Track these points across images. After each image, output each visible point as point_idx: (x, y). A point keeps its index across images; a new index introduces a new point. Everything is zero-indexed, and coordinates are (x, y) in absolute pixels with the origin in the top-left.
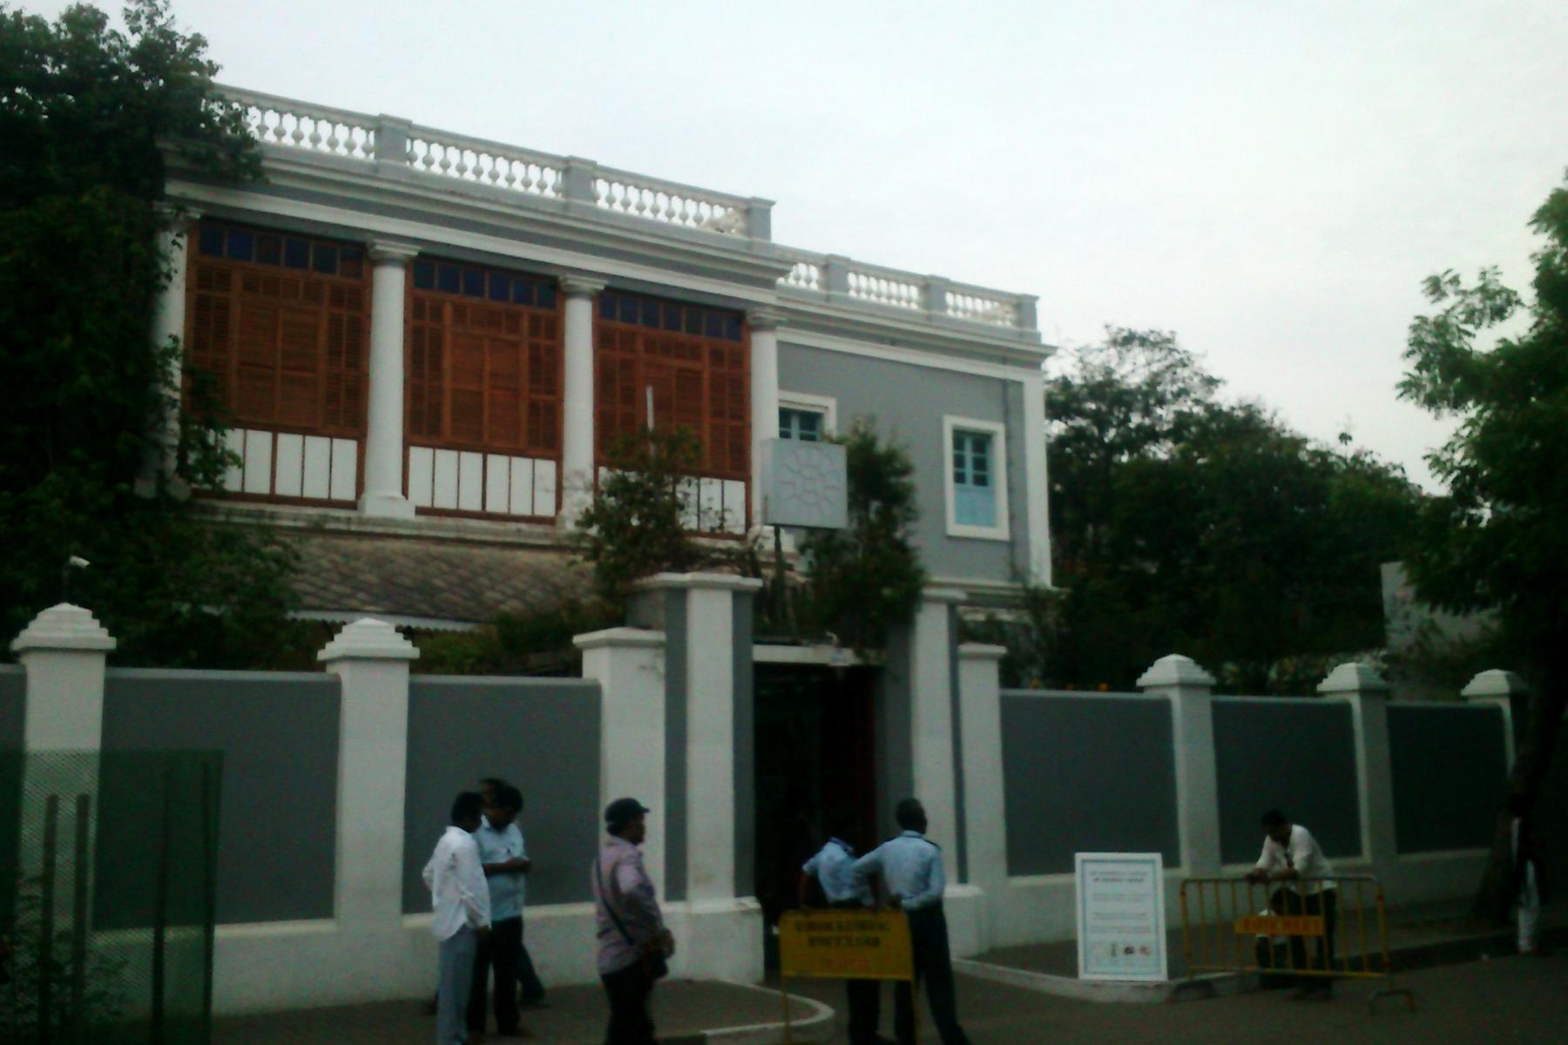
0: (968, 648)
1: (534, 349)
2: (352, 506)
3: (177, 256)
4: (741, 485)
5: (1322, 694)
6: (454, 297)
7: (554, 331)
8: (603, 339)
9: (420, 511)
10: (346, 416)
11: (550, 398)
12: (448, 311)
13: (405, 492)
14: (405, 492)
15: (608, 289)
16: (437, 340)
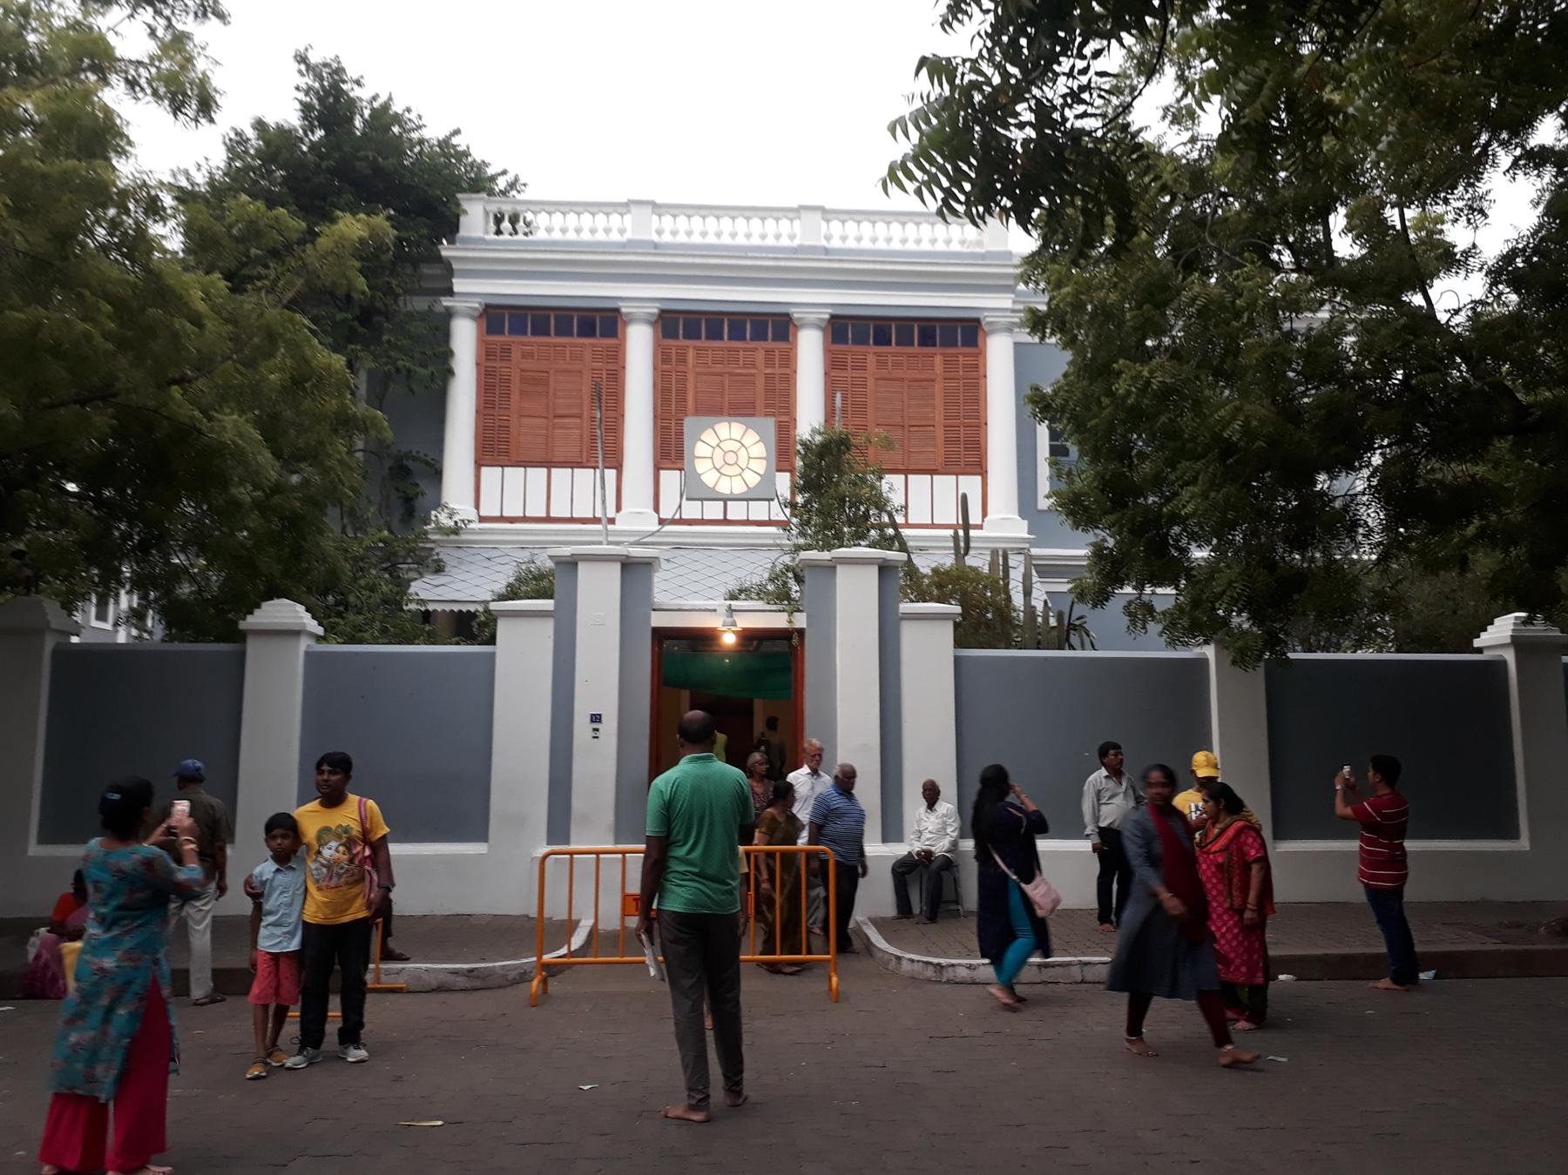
0: (906, 607)
1: (769, 378)
2: (612, 521)
3: (465, 339)
4: (614, 472)
5: (1480, 650)
6: (697, 343)
7: (789, 360)
8: (833, 365)
9: (662, 522)
10: (605, 451)
11: (784, 418)
12: (691, 354)
13: (657, 509)
14: (657, 509)
15: (833, 317)
16: (683, 381)
